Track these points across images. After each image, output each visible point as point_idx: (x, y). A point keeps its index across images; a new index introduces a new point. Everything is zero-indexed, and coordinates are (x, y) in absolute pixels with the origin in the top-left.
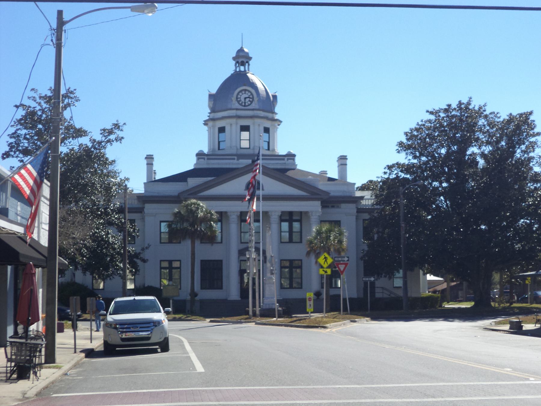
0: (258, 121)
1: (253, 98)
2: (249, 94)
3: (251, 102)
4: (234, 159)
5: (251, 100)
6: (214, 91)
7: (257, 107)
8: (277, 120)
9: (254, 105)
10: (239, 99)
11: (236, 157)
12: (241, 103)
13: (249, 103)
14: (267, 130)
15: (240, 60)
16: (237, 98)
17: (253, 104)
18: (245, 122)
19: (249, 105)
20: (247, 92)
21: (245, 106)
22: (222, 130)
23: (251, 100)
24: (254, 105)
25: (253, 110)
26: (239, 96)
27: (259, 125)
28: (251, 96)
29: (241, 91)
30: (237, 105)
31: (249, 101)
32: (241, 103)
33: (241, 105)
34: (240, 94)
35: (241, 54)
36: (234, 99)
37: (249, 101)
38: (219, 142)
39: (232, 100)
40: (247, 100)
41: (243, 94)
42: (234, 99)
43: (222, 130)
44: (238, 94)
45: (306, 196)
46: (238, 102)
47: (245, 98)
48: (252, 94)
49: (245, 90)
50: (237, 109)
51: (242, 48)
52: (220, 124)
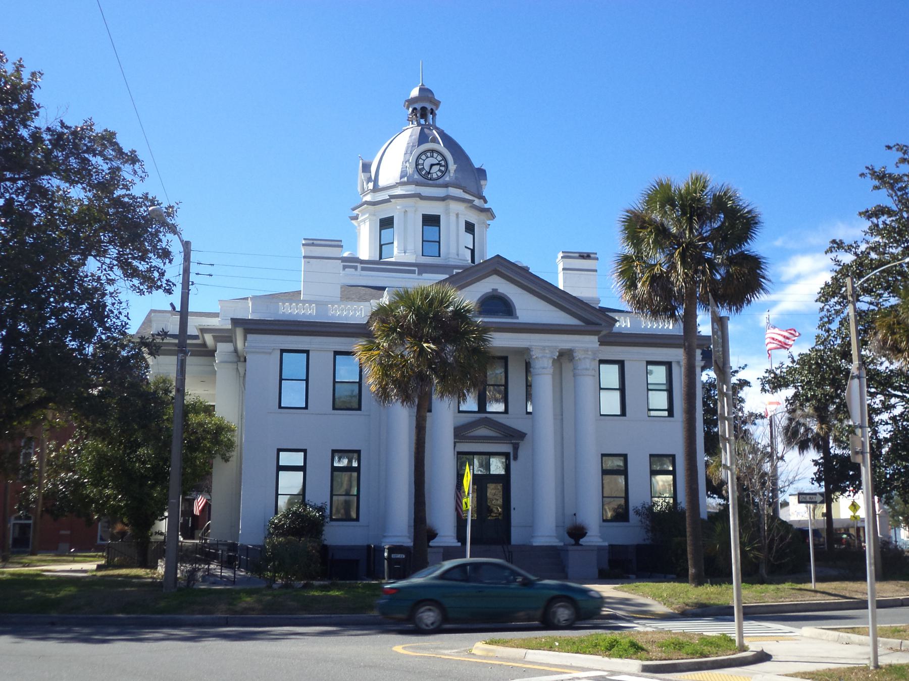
0: (455, 206)
1: (446, 166)
2: (440, 158)
3: (444, 173)
5: (443, 169)
8: (488, 210)
10: (420, 167)
13: (439, 174)
19: (439, 178)
20: (435, 155)
23: (443, 169)
25: (446, 186)
26: (421, 161)
27: (457, 215)
28: (443, 163)
31: (440, 170)
34: (423, 157)
37: (440, 170)
38: (381, 246)
40: (435, 168)
41: (427, 157)
47: (432, 165)
48: (444, 159)
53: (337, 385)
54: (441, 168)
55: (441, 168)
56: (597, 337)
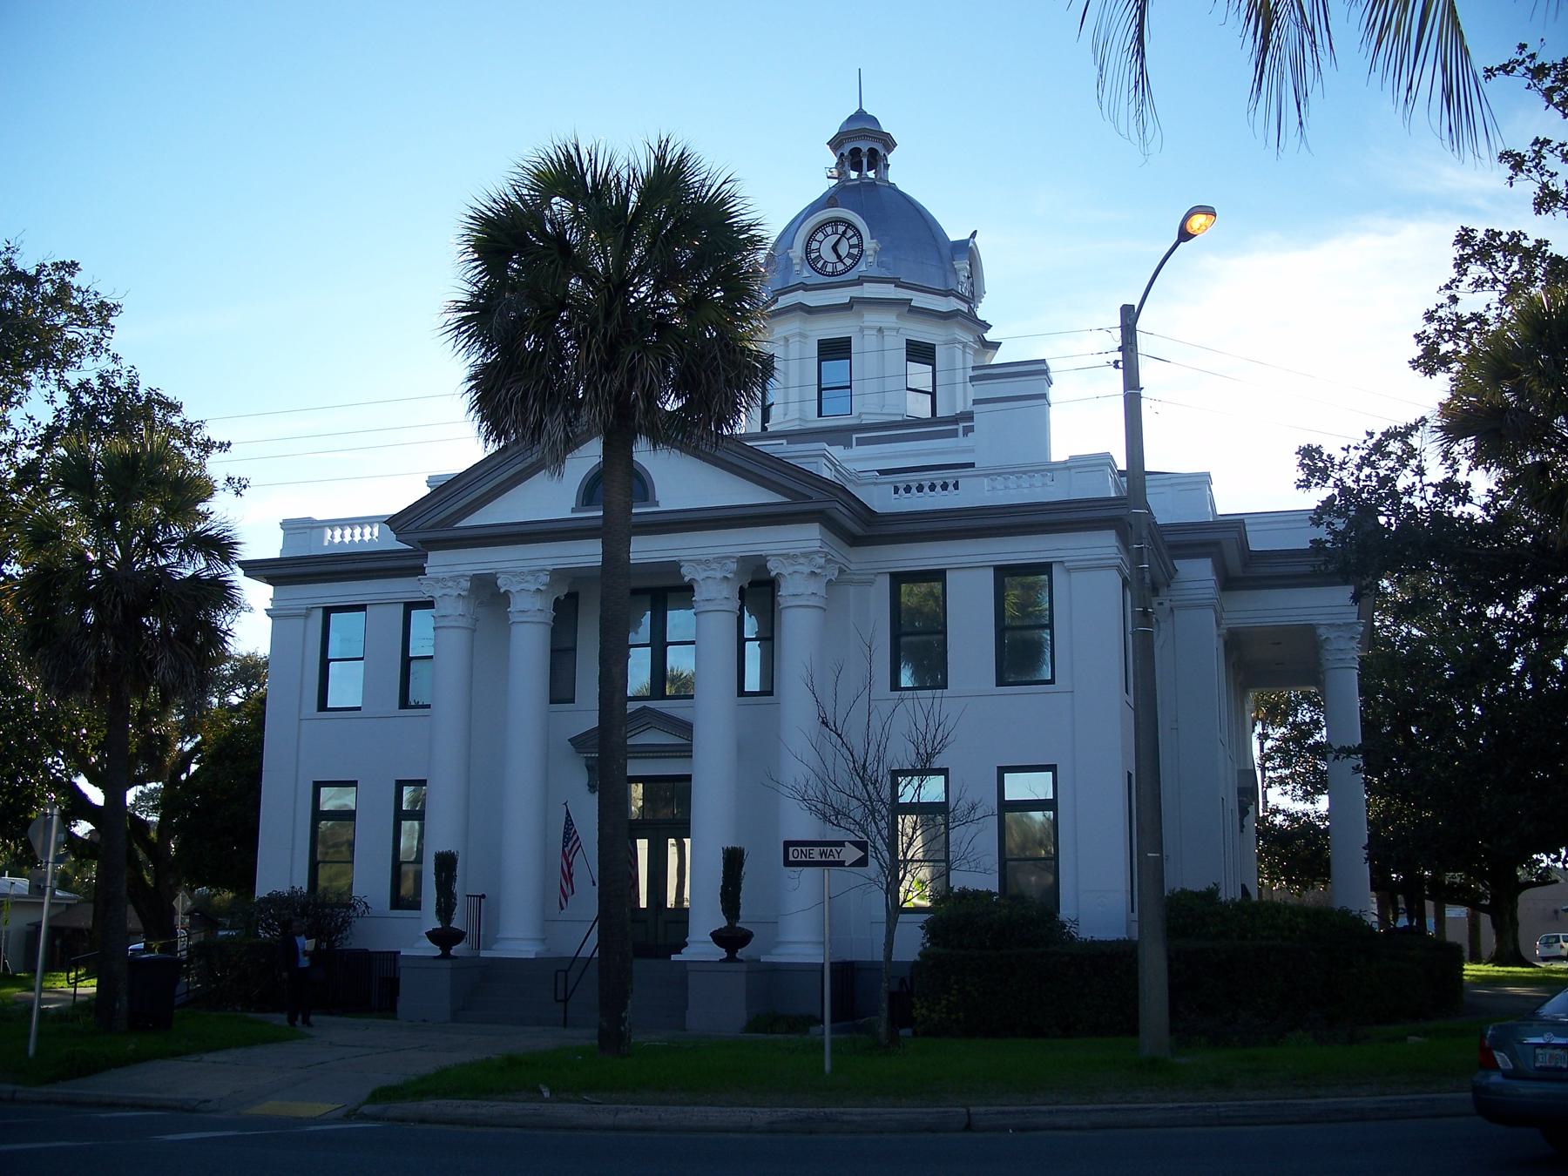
0: (873, 318)
3: (856, 259)
7: (875, 272)
9: (863, 268)
10: (813, 256)
12: (819, 265)
15: (846, 150)
16: (808, 251)
17: (862, 267)
18: (833, 328)
21: (833, 274)
26: (815, 245)
30: (807, 274)
32: (819, 265)
33: (821, 272)
34: (820, 236)
40: (843, 249)
44: (811, 238)
46: (812, 263)
50: (805, 287)
53: (414, 665)
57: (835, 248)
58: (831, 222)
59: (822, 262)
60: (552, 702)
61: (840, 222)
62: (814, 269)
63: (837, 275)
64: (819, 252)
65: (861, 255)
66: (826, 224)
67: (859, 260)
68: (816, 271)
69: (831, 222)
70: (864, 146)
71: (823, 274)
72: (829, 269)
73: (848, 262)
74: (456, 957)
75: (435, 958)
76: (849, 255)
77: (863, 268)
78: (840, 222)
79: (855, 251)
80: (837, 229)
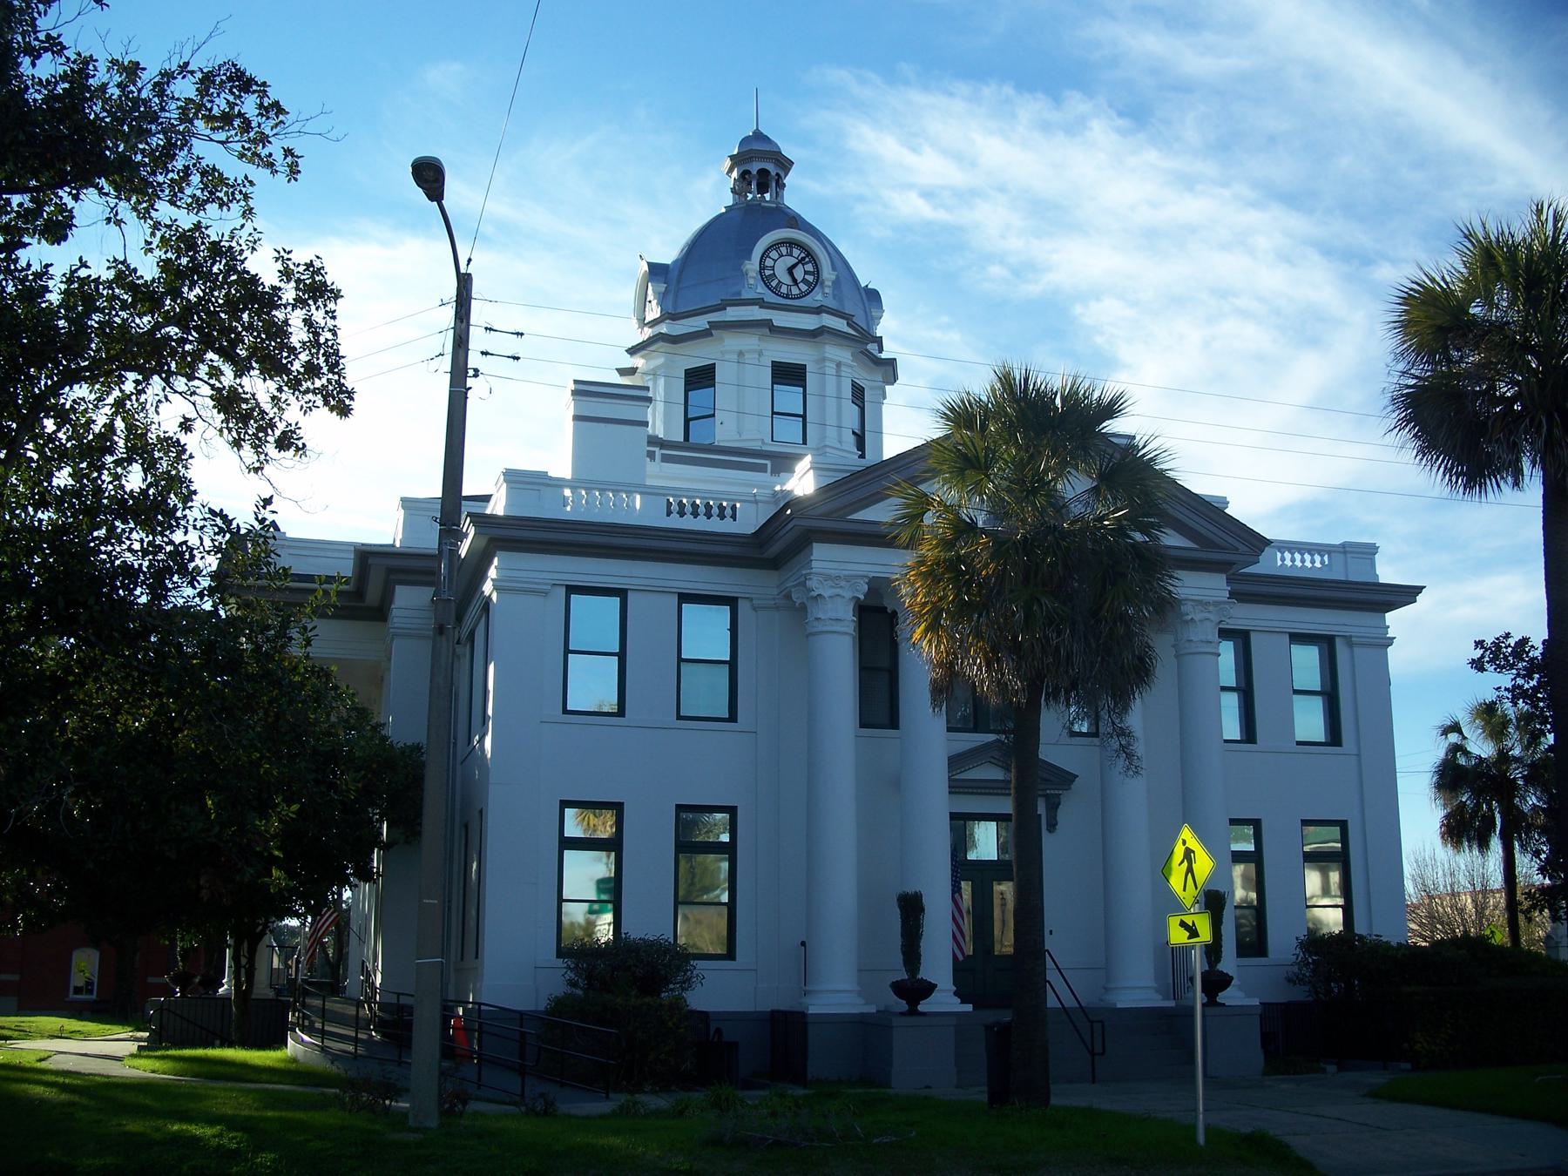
3: (812, 287)
4: (762, 469)
5: (810, 278)
6: (668, 254)
10: (768, 272)
11: (768, 462)
12: (774, 284)
14: (858, 394)
16: (762, 268)
18: (791, 353)
19: (803, 295)
21: (787, 297)
22: (700, 378)
24: (819, 297)
25: (818, 310)
26: (769, 262)
29: (775, 246)
32: (774, 284)
33: (775, 291)
35: (757, 146)
36: (752, 266)
38: (687, 421)
39: (744, 275)
40: (799, 273)
41: (781, 256)
42: (752, 266)
43: (700, 378)
44: (765, 255)
45: (1180, 548)
46: (766, 281)
47: (790, 270)
49: (791, 243)
50: (761, 303)
51: (757, 129)
52: (697, 356)
53: (684, 667)
54: (807, 277)
55: (807, 277)
56: (1224, 576)
57: (790, 270)
58: (786, 243)
59: (776, 281)
60: (863, 725)
61: (796, 245)
62: (768, 287)
63: (792, 298)
64: (773, 270)
65: (817, 283)
66: (780, 243)
67: (814, 288)
68: (770, 289)
69: (786, 243)
70: (755, 168)
71: (777, 294)
72: (784, 290)
73: (804, 287)
74: (924, 1014)
75: (902, 1014)
76: (804, 281)
77: (819, 297)
78: (796, 245)
79: (810, 278)
80: (791, 251)
